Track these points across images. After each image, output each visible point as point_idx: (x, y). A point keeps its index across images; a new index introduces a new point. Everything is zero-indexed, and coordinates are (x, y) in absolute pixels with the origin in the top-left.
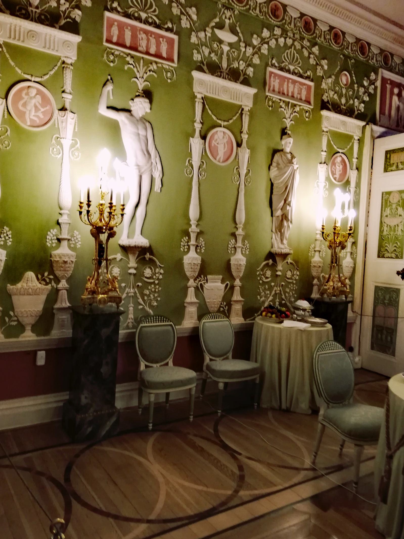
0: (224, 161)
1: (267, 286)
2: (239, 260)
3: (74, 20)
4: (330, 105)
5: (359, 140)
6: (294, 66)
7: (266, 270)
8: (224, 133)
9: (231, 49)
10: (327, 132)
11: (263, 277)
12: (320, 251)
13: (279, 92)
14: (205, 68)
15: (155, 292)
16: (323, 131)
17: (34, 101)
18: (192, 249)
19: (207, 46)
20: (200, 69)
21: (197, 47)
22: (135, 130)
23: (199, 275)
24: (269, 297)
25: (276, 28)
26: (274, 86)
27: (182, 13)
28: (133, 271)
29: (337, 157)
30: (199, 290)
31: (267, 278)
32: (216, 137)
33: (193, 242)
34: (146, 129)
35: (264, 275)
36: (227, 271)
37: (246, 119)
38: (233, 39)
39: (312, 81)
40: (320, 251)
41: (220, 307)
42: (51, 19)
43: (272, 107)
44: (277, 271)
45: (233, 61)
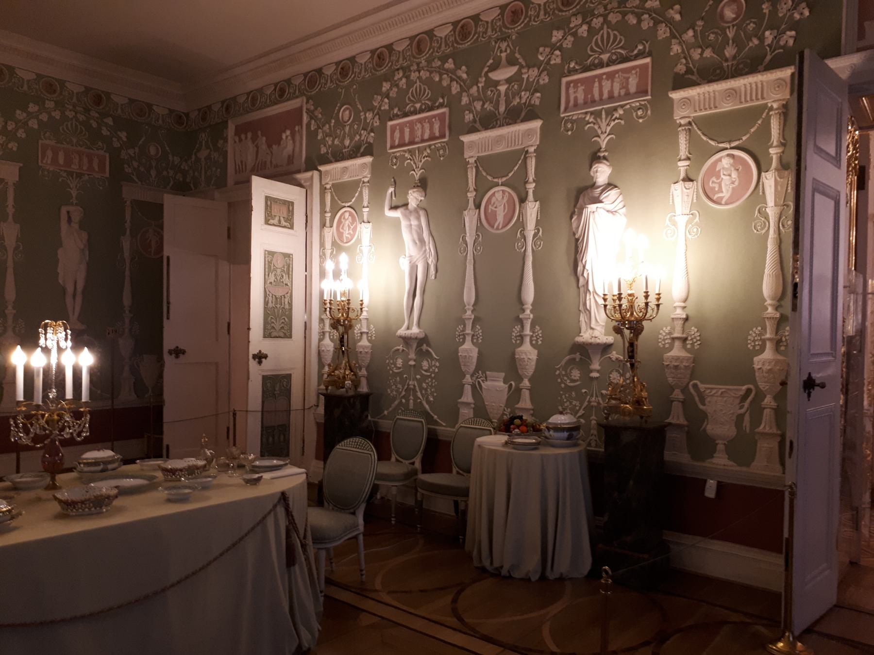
2: (528, 353)
3: (370, 144)
4: (693, 74)
5: (785, 106)
6: (609, 52)
7: (572, 369)
8: (503, 191)
10: (690, 123)
12: (685, 339)
13: (585, 103)
15: (431, 386)
16: (681, 125)
17: (347, 222)
18: (468, 339)
19: (479, 99)
20: (472, 130)
21: (469, 108)
22: (408, 223)
23: (476, 370)
24: (578, 411)
25: (573, 19)
26: (576, 98)
27: (452, 80)
28: (412, 363)
29: (720, 160)
30: (476, 390)
31: (573, 381)
32: (493, 200)
33: (468, 331)
34: (418, 218)
35: (568, 375)
36: (512, 369)
37: (532, 164)
38: (511, 71)
39: (650, 54)
40: (685, 339)
41: (503, 414)
42: (354, 153)
43: (572, 129)
44: (591, 371)
45: (513, 98)
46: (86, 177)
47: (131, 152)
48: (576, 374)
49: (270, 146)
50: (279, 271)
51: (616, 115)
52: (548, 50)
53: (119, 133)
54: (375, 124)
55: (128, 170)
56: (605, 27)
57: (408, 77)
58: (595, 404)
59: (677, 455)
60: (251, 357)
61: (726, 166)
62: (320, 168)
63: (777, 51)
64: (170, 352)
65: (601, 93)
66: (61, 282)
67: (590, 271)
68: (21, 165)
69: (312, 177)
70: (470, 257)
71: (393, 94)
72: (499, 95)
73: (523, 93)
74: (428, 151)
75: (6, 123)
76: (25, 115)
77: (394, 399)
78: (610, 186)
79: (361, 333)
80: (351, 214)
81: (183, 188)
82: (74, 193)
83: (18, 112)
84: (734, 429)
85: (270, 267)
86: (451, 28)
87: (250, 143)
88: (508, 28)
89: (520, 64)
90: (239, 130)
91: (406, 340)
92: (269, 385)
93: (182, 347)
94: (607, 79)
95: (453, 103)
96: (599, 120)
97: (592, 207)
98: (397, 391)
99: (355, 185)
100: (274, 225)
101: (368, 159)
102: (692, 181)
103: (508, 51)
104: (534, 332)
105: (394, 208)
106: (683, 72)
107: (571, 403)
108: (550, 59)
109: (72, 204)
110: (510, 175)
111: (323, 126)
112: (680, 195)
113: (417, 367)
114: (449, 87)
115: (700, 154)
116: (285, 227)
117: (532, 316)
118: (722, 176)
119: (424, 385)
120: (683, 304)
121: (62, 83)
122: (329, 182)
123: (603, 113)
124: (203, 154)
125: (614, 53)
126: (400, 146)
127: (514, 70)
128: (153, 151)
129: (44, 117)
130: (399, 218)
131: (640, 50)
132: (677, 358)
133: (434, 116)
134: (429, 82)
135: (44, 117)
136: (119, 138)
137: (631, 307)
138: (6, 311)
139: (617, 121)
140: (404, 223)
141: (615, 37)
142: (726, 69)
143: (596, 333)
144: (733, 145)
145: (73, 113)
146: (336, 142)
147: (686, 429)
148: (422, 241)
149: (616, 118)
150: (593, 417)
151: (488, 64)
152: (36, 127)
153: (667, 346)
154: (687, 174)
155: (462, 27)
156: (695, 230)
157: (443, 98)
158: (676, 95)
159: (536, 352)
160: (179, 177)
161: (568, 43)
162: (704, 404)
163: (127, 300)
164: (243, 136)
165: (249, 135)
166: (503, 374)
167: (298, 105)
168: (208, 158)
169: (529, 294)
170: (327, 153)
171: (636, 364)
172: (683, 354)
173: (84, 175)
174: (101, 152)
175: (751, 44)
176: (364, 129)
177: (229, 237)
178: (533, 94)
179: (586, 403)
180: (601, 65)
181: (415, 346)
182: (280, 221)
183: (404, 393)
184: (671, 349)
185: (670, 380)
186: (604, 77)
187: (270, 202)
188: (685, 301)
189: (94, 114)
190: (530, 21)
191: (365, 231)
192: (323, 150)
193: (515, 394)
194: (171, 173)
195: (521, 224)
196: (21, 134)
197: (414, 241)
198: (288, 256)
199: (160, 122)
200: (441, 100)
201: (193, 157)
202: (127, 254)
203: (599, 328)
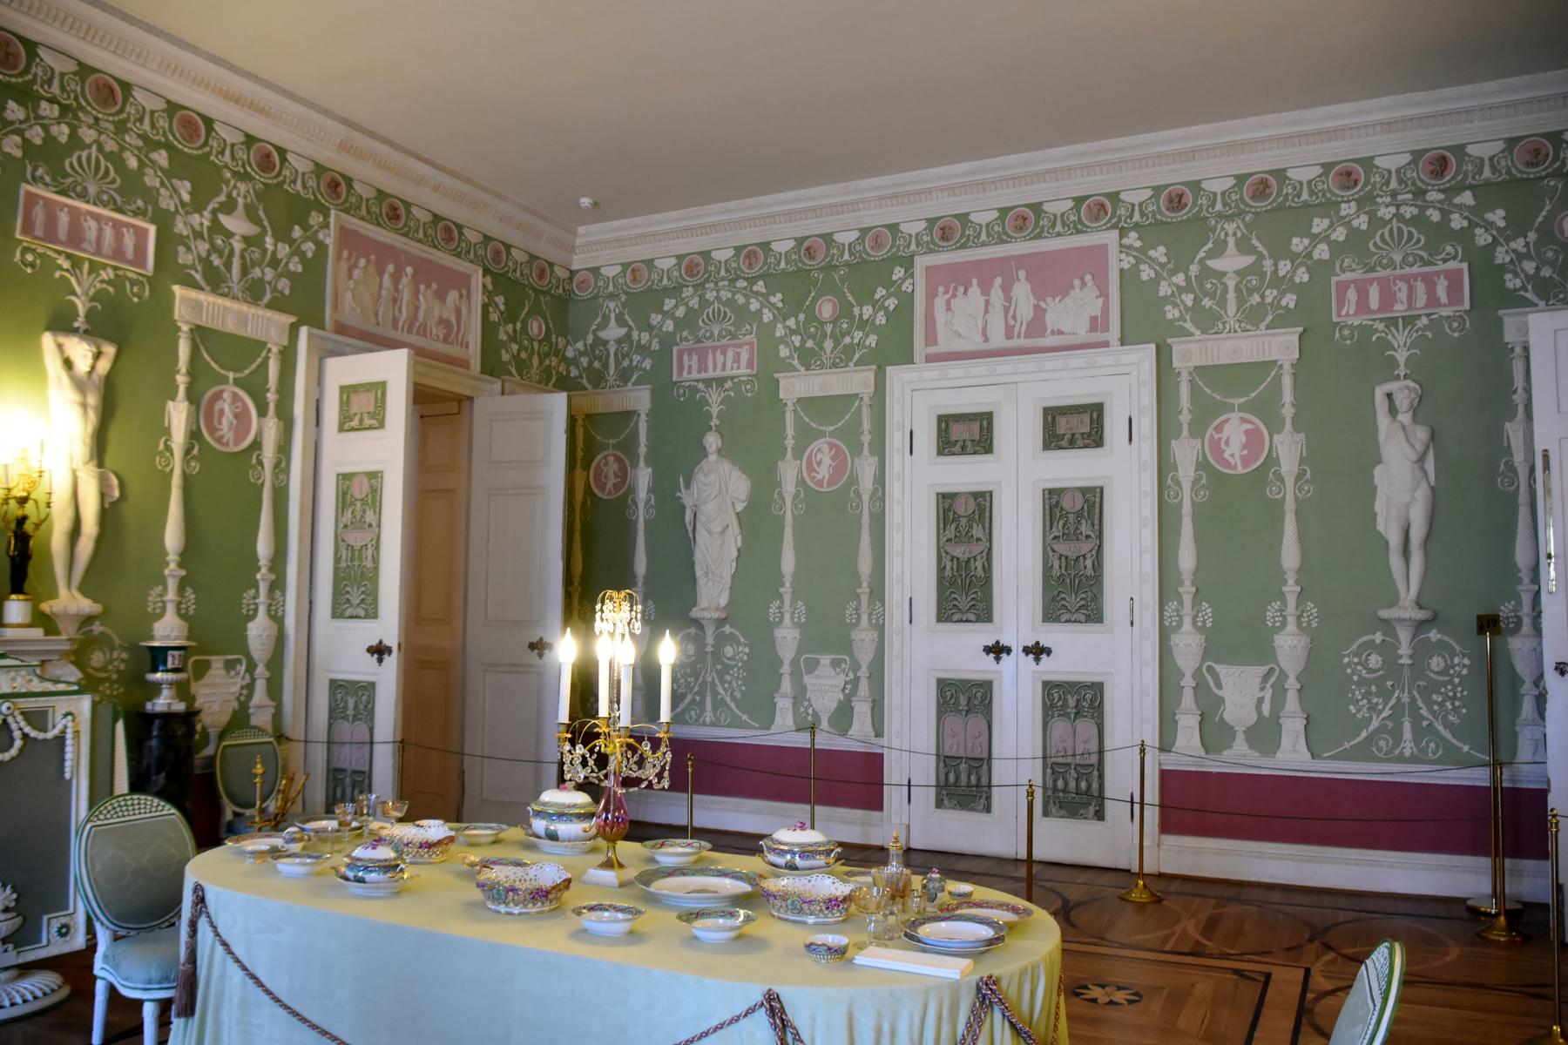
47: (1519, 244)
53: (1489, 216)
55: (1511, 282)
66: (1380, 527)
75: (1276, 265)
82: (1401, 356)
83: (1296, 240)
109: (1398, 378)
121: (1367, 163)
129: (1340, 234)
136: (1489, 226)
138: (1285, 589)
145: (1393, 210)
152: (1326, 256)
173: (1419, 317)
174: (1451, 265)
189: (1433, 196)
196: (1302, 276)
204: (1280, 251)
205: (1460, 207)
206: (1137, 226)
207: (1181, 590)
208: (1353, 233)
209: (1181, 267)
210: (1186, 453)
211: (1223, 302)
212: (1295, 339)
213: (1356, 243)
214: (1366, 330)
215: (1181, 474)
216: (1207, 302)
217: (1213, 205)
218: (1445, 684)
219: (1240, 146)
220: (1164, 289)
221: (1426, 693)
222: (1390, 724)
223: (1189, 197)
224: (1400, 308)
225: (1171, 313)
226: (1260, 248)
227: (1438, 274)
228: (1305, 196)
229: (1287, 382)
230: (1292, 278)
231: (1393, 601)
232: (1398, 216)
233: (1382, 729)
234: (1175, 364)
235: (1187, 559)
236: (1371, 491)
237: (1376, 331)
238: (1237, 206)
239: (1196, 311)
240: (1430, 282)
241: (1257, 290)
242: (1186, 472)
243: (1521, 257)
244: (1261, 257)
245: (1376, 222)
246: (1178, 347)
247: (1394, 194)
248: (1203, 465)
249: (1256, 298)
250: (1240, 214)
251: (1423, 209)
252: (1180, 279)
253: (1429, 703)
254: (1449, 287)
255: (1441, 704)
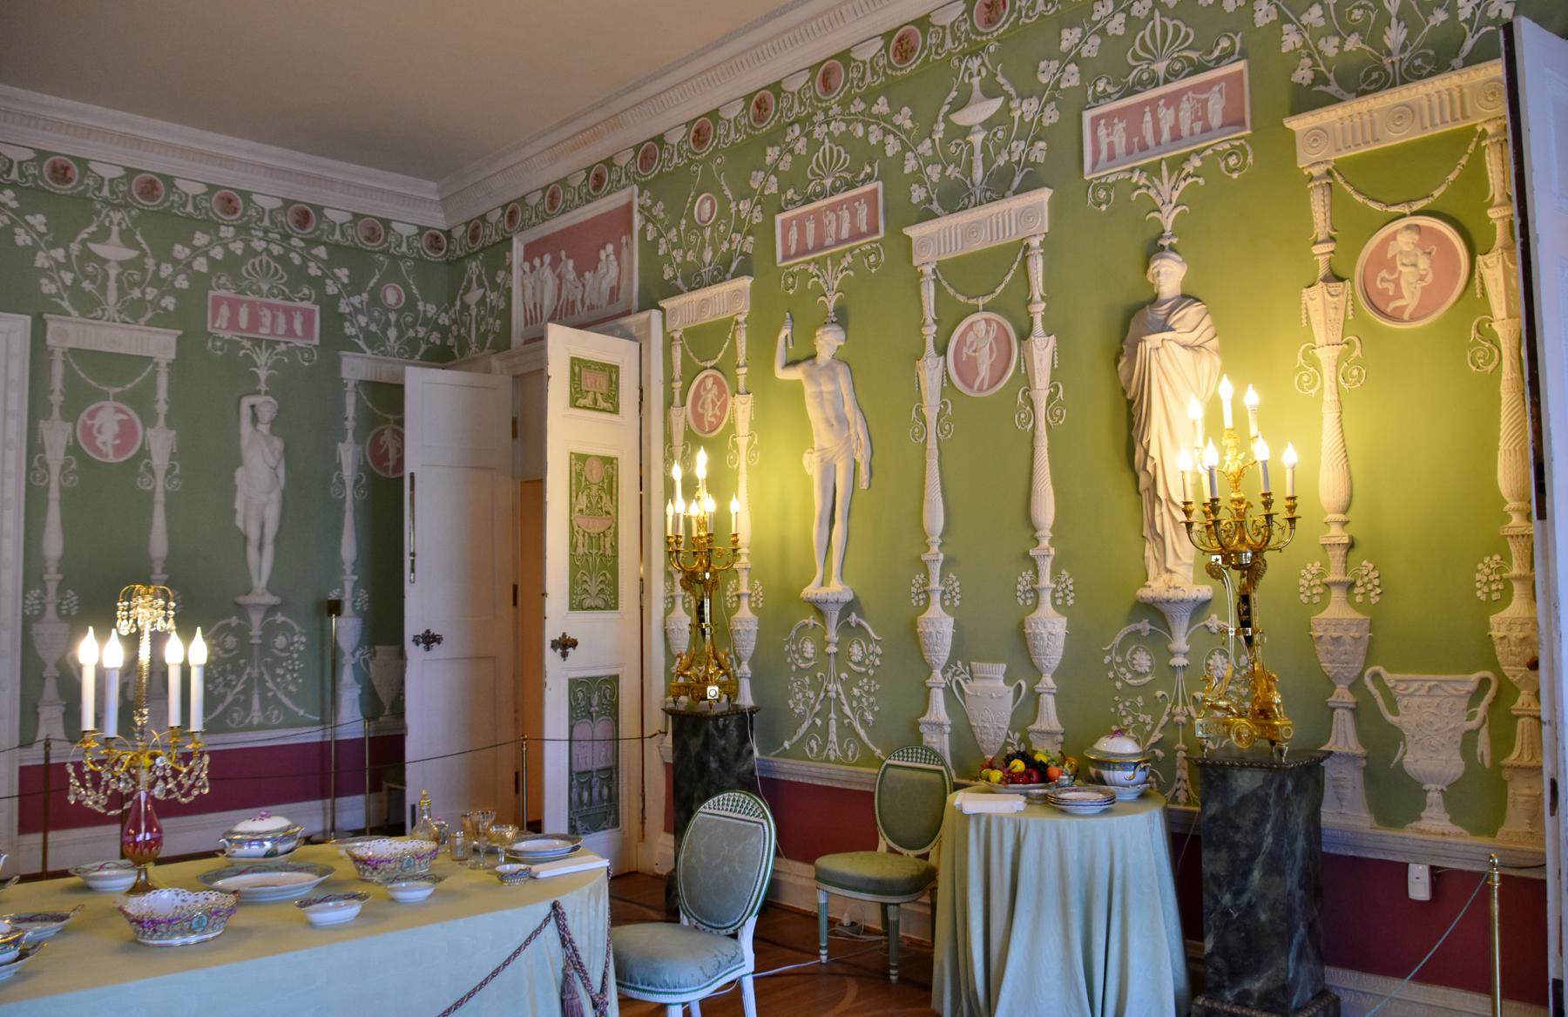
0: (991, 386)
1: (1139, 699)
3: (746, 254)
4: (1327, 83)
7: (1134, 652)
8: (988, 322)
9: (989, 130)
10: (1329, 173)
11: (1123, 670)
12: (1352, 585)
13: (1129, 152)
14: (935, 206)
15: (869, 693)
16: (1312, 178)
21: (918, 178)
23: (952, 661)
24: (1150, 733)
26: (1111, 146)
27: (886, 132)
28: (832, 649)
29: (1393, 237)
31: (1137, 674)
32: (970, 337)
33: (935, 584)
34: (834, 379)
37: (1037, 268)
40: (1352, 585)
41: (1007, 743)
42: (722, 273)
44: (1173, 654)
45: (998, 153)
46: (282, 347)
47: (356, 300)
48: (1143, 661)
49: (580, 275)
50: (595, 488)
51: (1189, 168)
52: (1055, 64)
54: (755, 221)
55: (349, 330)
56: (1157, 13)
57: (809, 135)
58: (1183, 719)
59: (1347, 816)
60: (548, 644)
61: (1406, 248)
62: (663, 304)
63: (1483, 30)
64: (416, 640)
65: (1157, 133)
66: (239, 523)
67: (1157, 460)
68: (180, 332)
69: (649, 319)
70: (932, 444)
71: (785, 166)
72: (971, 153)
73: (1014, 144)
74: (849, 259)
75: (158, 266)
76: (188, 251)
77: (802, 718)
78: (1186, 298)
79: (738, 596)
80: (716, 381)
81: (440, 357)
83: (178, 247)
84: (1457, 758)
85: (579, 482)
86: (881, 43)
87: (548, 272)
88: (982, 34)
89: (1005, 94)
90: (532, 251)
91: (818, 608)
92: (580, 695)
93: (434, 631)
94: (1167, 106)
95: (891, 171)
96: (1156, 181)
97: (1153, 340)
98: (806, 703)
99: (724, 328)
100: (585, 407)
101: (746, 282)
102: (1342, 280)
103: (984, 73)
104: (1057, 583)
105: (792, 363)
106: (1307, 81)
107: (1135, 718)
108: (1059, 81)
109: (258, 393)
110: (999, 290)
111: (668, 230)
112: (1321, 308)
113: (842, 657)
114: (882, 144)
115: (1351, 230)
116: (604, 410)
117: (1052, 551)
118: (1400, 268)
119: (856, 692)
120: (1342, 517)
122: (678, 327)
123: (1164, 167)
124: (475, 295)
125: (1177, 59)
126: (797, 255)
127: (997, 103)
128: (391, 297)
129: (218, 253)
130: (799, 381)
131: (1223, 49)
132: (1338, 623)
133: (857, 198)
134: (845, 139)
135: (218, 253)
136: (336, 279)
137: (1241, 525)
139: (1190, 180)
140: (809, 390)
141: (1177, 30)
142: (1390, 70)
143: (1177, 580)
144: (1417, 206)
145: (264, 244)
146: (690, 256)
147: (1364, 763)
148: (842, 421)
149: (1188, 175)
150: (1180, 745)
151: (949, 99)
152: (204, 269)
153: (1316, 599)
154: (1331, 269)
155: (899, 41)
156: (1355, 372)
157: (871, 166)
158: (1298, 124)
159: (1064, 620)
160: (435, 337)
161: (1092, 48)
162: (1396, 713)
163: (348, 550)
164: (537, 262)
165: (547, 258)
166: (1003, 667)
167: (624, 201)
168: (482, 302)
169: (1046, 510)
170: (675, 277)
171: (1257, 638)
172: (1349, 614)
175: (1432, 22)
176: (736, 231)
177: (515, 435)
178: (1032, 144)
179: (1165, 718)
180: (1154, 82)
181: (835, 617)
182: (595, 400)
183: (818, 707)
184: (1323, 604)
185: (1327, 666)
186: (1162, 102)
187: (579, 367)
188: (1346, 510)
189: (295, 242)
190: (1020, 17)
191: (742, 409)
192: (668, 273)
193: (1028, 705)
194: (422, 332)
195: (1025, 379)
196: (182, 283)
197: (827, 421)
198: (609, 462)
199: (404, 248)
200: (869, 170)
201: (458, 303)
202: (348, 473)
203: (1181, 570)
204: (164, 255)
205: (316, 257)
206: (14, 185)
207: (46, 577)
208: (229, 254)
209: (61, 241)
210: (56, 435)
211: (103, 289)
212: (173, 341)
213: (230, 264)
214: (235, 345)
215: (49, 456)
216: (87, 285)
217: (100, 189)
218: (286, 659)
219: (136, 142)
220: (41, 260)
221: (271, 668)
222: (242, 697)
223: (75, 172)
224: (264, 331)
225: (48, 288)
226: (144, 246)
227: (296, 309)
228: (190, 208)
229: (163, 381)
230: (172, 283)
231: (248, 591)
232: (267, 250)
233: (235, 702)
234: (51, 340)
235: (53, 545)
236: (232, 491)
237: (243, 348)
238: (124, 198)
239: (74, 290)
240: (289, 314)
241: (139, 285)
242: (55, 456)
243: (357, 311)
244: (143, 254)
245: (250, 252)
246: (54, 325)
247: (266, 231)
248: (73, 449)
249: (136, 293)
250: (126, 207)
251: (288, 250)
252: (59, 254)
253: (274, 676)
254: (304, 323)
255: (283, 677)
